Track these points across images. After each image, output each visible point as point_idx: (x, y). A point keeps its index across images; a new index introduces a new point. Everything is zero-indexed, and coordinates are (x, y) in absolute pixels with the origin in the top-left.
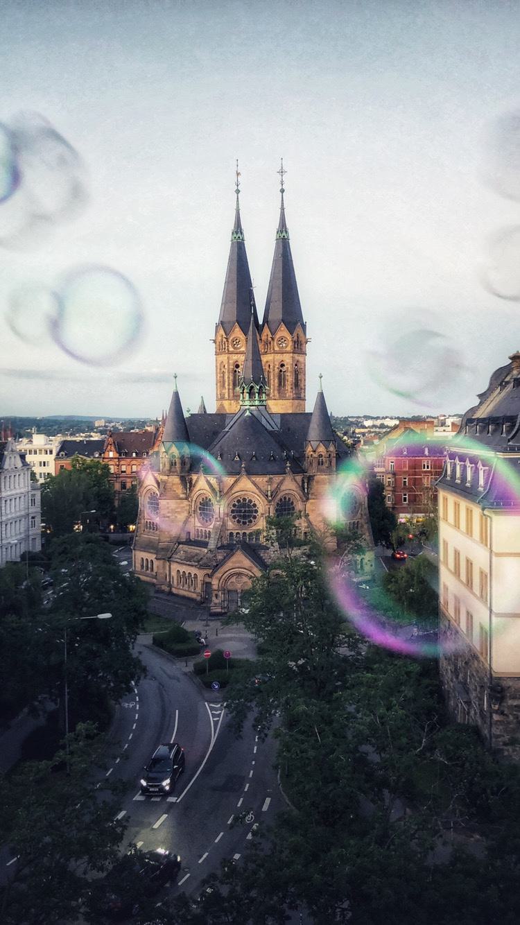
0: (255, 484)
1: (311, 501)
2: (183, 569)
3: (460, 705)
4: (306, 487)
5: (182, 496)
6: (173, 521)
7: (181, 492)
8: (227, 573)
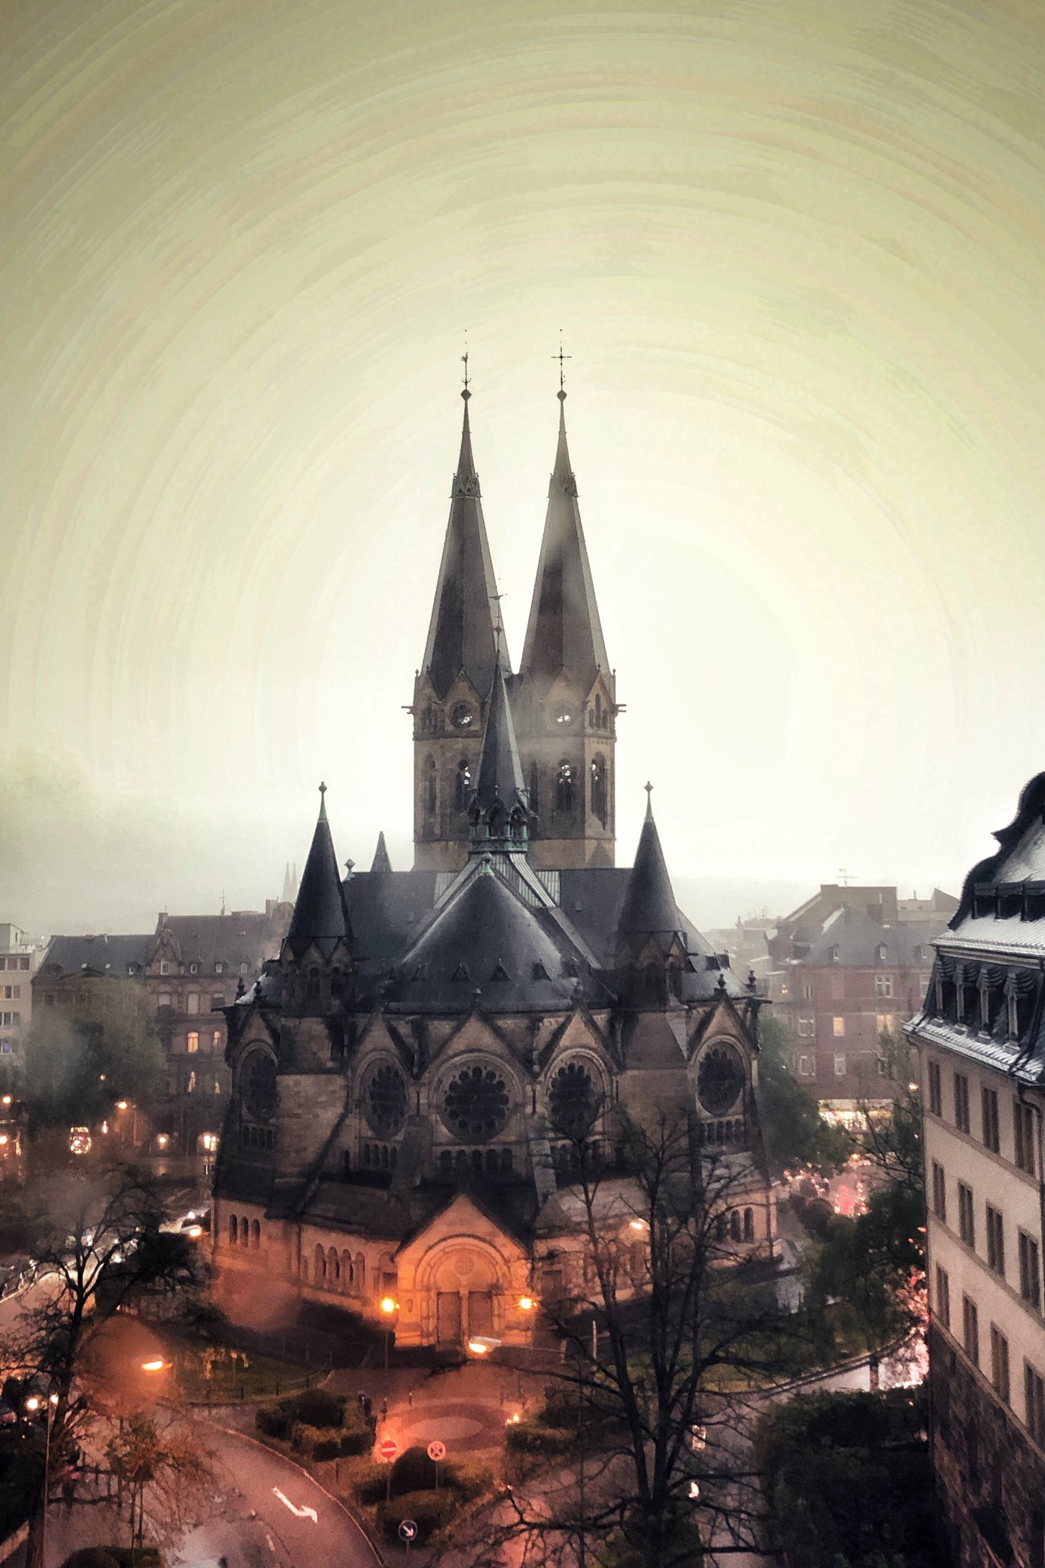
0: (498, 1032)
2: (331, 1241)
3: (986, 1562)
5: (330, 1065)
6: (308, 1127)
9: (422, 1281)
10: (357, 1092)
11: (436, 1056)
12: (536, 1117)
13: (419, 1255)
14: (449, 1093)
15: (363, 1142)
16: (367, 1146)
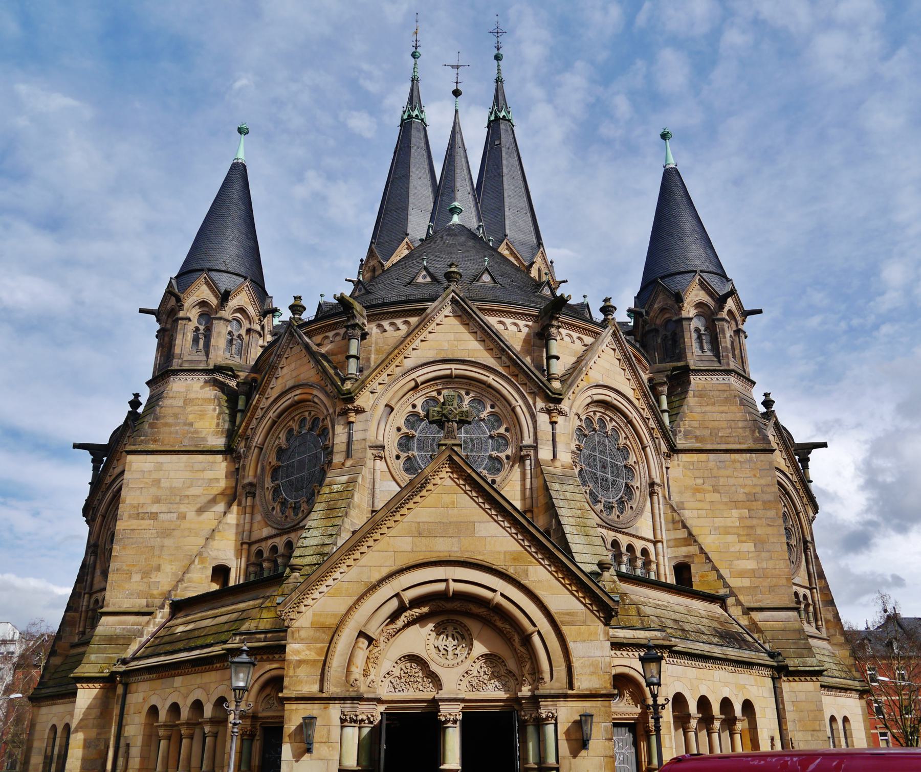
1: (684, 457)
4: (665, 406)
7: (213, 426)
8: (387, 590)
9: (348, 672)
10: (251, 473)
11: (385, 363)
12: (558, 464)
13: (340, 606)
14: (404, 430)
15: (254, 548)
16: (260, 553)
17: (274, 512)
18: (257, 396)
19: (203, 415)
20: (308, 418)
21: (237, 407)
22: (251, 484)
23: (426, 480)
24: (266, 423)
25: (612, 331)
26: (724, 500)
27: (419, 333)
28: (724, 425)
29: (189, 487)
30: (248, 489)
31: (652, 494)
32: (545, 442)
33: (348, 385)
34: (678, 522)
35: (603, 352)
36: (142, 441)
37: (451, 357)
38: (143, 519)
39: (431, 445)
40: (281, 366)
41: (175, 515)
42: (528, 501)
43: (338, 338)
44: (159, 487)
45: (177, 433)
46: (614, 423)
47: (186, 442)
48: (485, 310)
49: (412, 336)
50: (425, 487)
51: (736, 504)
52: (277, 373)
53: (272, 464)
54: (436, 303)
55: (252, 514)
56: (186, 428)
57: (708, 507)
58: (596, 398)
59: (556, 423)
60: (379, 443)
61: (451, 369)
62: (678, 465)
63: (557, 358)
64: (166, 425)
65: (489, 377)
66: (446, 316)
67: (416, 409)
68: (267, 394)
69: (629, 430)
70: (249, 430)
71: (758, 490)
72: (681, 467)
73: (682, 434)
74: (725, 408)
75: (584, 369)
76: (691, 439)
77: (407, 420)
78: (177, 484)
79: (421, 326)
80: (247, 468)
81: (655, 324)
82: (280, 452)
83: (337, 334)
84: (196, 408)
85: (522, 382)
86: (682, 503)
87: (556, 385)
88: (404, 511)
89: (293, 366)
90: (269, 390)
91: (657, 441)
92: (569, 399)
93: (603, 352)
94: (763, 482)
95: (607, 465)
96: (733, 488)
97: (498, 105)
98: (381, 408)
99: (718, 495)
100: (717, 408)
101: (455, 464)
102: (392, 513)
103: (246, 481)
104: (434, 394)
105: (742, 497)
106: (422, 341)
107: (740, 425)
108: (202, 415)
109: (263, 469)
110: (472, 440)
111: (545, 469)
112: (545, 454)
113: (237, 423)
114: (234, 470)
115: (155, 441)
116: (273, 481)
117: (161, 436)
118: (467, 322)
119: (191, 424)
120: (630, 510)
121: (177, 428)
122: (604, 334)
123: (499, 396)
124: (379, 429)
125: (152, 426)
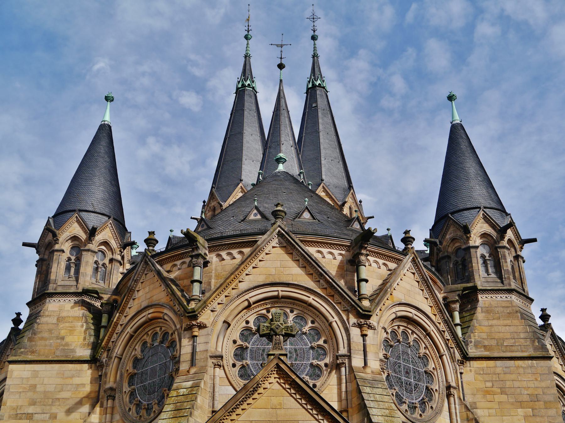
1: (475, 364)
4: (458, 321)
10: (112, 379)
11: (223, 286)
12: (368, 370)
14: (239, 342)
17: (131, 413)
18: (118, 314)
19: (72, 330)
20: (160, 333)
21: (101, 324)
22: (111, 389)
23: (258, 385)
24: (124, 337)
25: (411, 258)
26: (511, 400)
27: (251, 261)
28: (508, 336)
29: (59, 391)
30: (109, 393)
31: (449, 395)
32: (357, 352)
33: (193, 305)
34: (472, 419)
35: (404, 275)
36: (22, 353)
37: (278, 281)
38: (20, 419)
39: (261, 355)
40: (137, 289)
41: (48, 415)
42: (344, 402)
43: (185, 266)
44: (35, 392)
45: (51, 345)
46: (415, 336)
47: (58, 353)
48: (305, 241)
49: (245, 264)
50: (256, 391)
51: (521, 404)
52: (134, 295)
53: (129, 372)
54: (265, 236)
55: (112, 414)
56: (59, 341)
57: (497, 406)
58: (400, 314)
59: (366, 335)
60: (218, 354)
61: (278, 291)
62: (471, 371)
63: (367, 281)
64: (42, 338)
65: (309, 297)
66: (273, 247)
67: (249, 324)
68: (125, 312)
69: (427, 341)
70: (111, 343)
71: (540, 391)
72: (473, 373)
73: (472, 344)
74: (508, 322)
75: (389, 290)
76: (481, 348)
77: (242, 334)
78: (51, 388)
79: (253, 255)
80: (108, 375)
81: (447, 252)
82: (136, 361)
83: (184, 263)
84: (67, 324)
85: (338, 302)
86: (475, 403)
87: (366, 303)
88: (239, 411)
89: (147, 289)
90: (127, 309)
91: (452, 350)
92: (377, 315)
93: (404, 275)
94: (543, 384)
95: (410, 371)
96: (518, 390)
97: (314, 76)
98: (220, 324)
99: (506, 396)
100: (501, 322)
101: (282, 371)
102: (229, 413)
103: (108, 386)
104: (264, 312)
105: (526, 398)
106: (254, 268)
107: (522, 335)
108: (72, 331)
109: (121, 376)
110: (296, 350)
111: (358, 375)
112: (357, 362)
113: (101, 337)
114: (98, 376)
115: (33, 352)
116: (130, 386)
117: (38, 348)
118: (291, 252)
119: (63, 338)
120: (430, 410)
121: (51, 341)
122: (405, 261)
123: (318, 313)
124: (218, 342)
125: (30, 340)
